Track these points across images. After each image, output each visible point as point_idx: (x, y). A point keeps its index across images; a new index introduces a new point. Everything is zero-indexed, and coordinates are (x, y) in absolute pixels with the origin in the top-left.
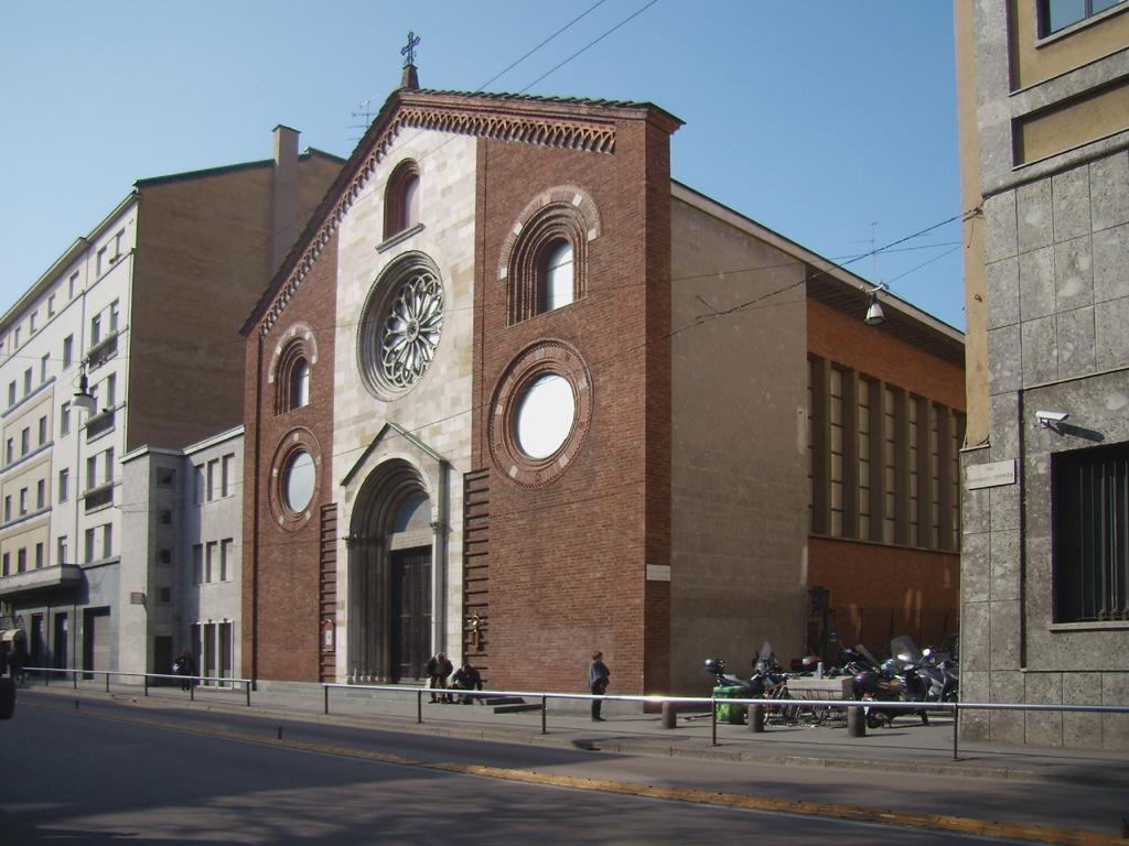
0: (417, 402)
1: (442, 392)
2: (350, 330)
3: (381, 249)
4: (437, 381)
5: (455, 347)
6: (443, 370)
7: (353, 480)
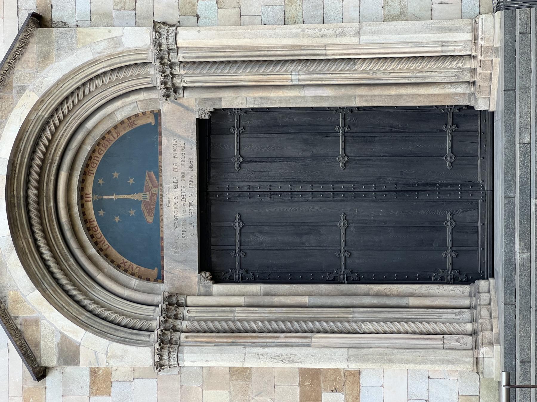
7: (29, 334)
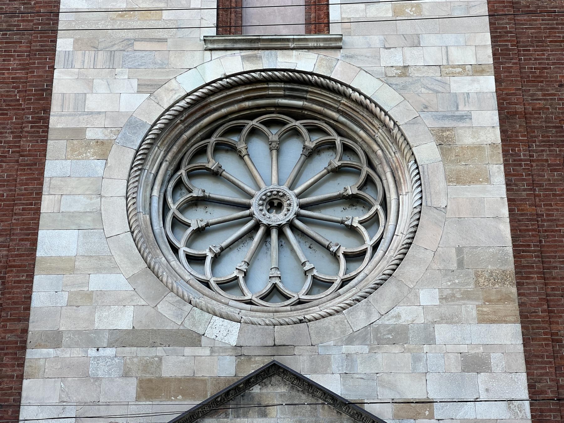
0: (350, 341)
1: (430, 340)
2: (104, 157)
3: (210, 45)
4: (406, 314)
5: (461, 264)
6: (428, 297)
